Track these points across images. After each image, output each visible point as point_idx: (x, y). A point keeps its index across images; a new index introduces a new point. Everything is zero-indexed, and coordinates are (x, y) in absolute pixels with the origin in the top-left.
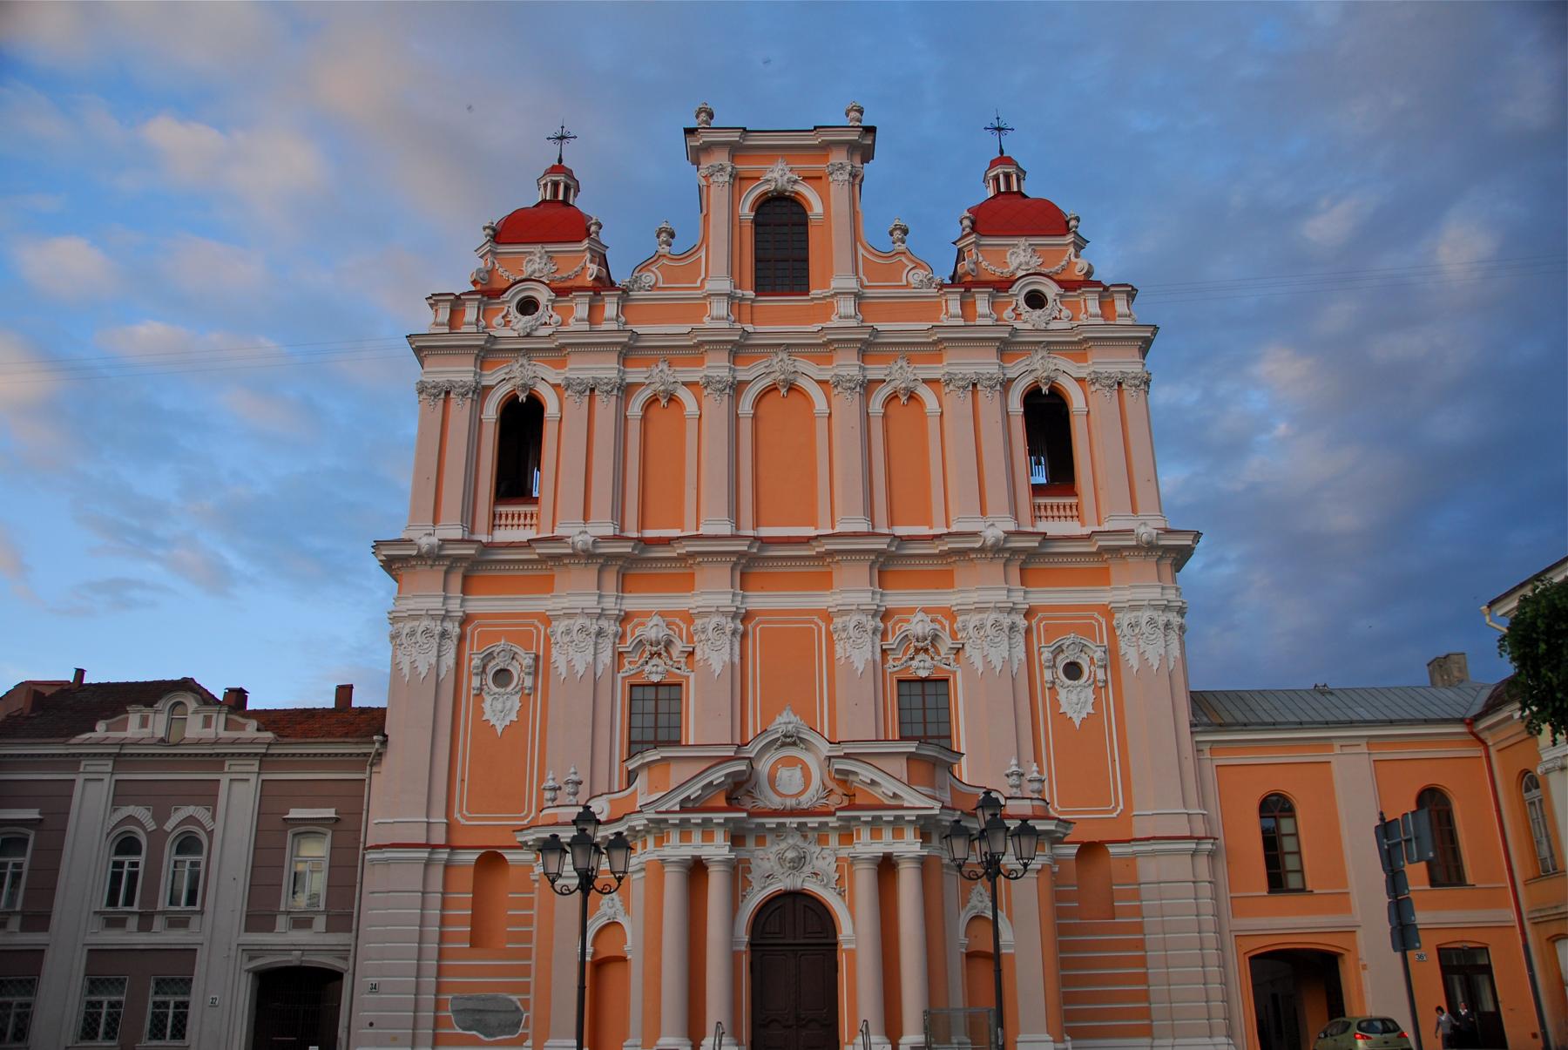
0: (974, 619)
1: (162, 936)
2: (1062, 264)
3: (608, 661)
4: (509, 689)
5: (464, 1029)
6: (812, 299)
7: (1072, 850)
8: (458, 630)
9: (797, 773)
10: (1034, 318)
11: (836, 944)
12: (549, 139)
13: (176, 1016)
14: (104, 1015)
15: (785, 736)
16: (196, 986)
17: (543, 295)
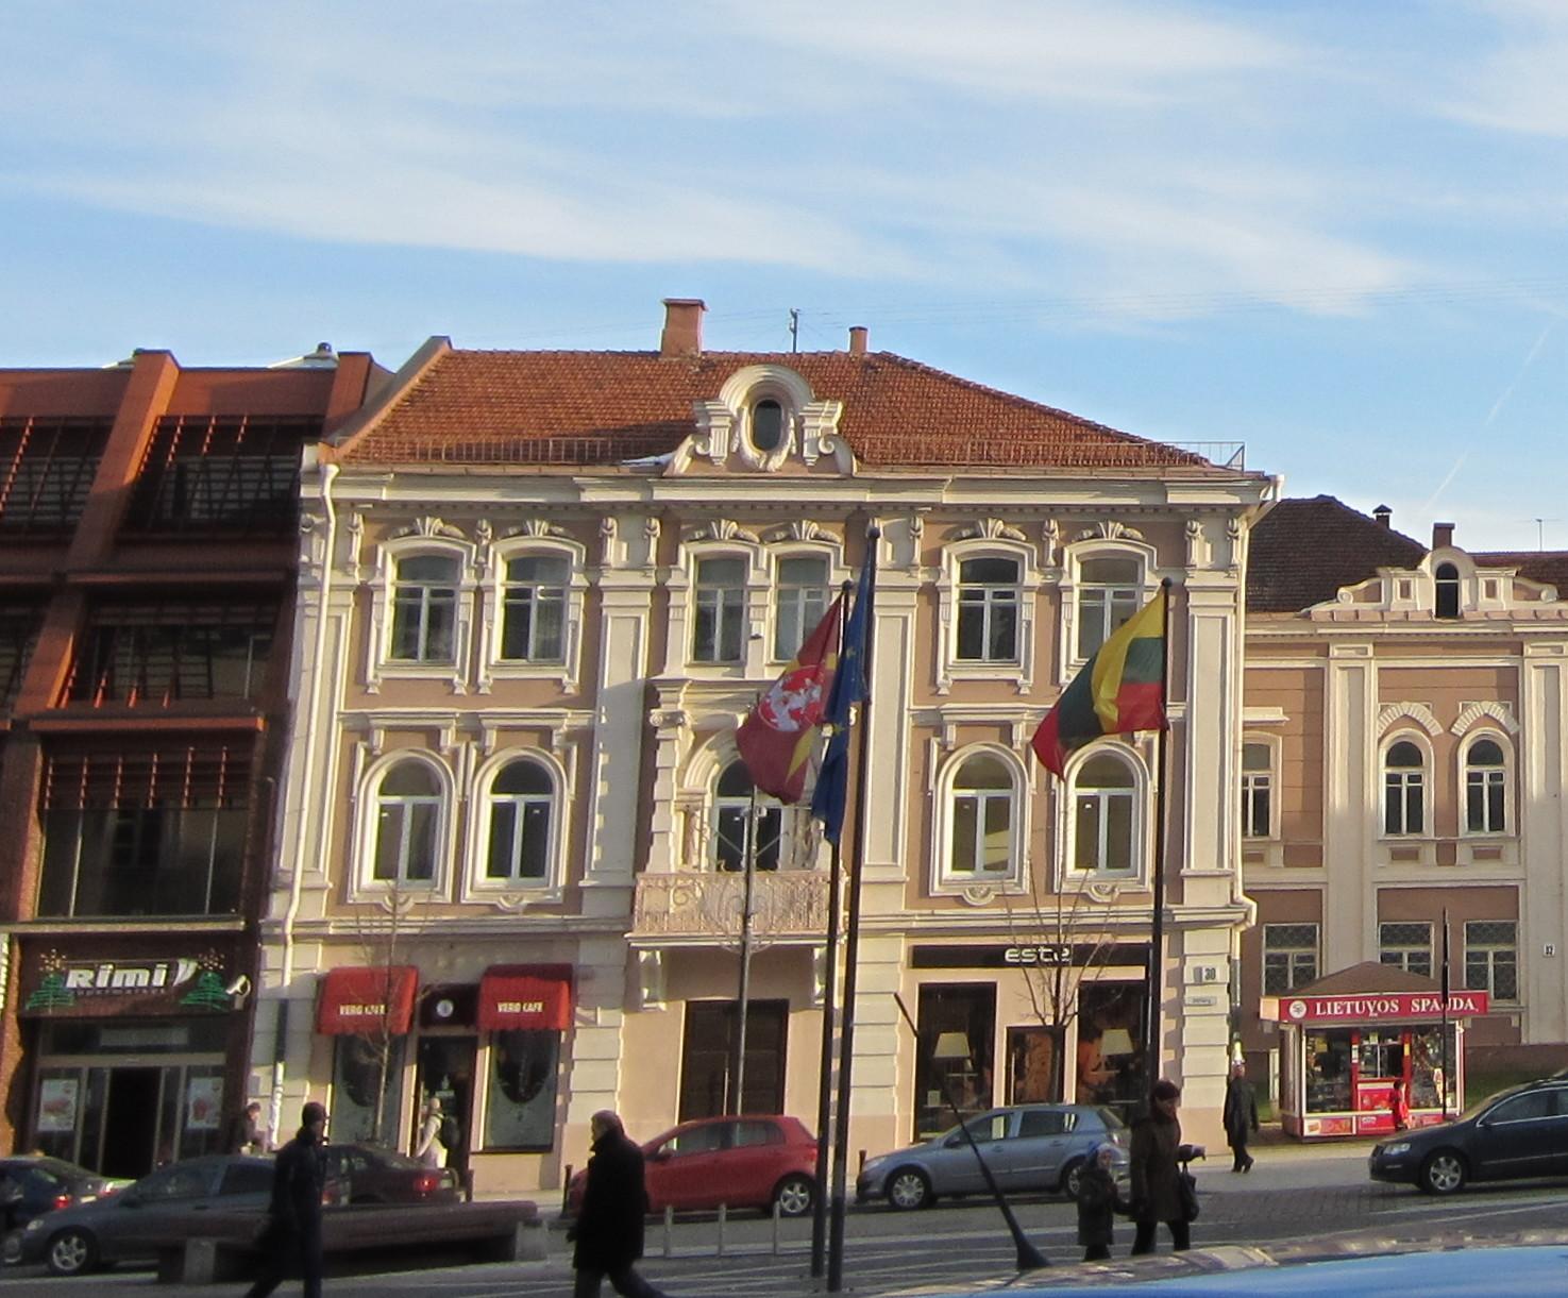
1: (1468, 871)
14: (1491, 969)
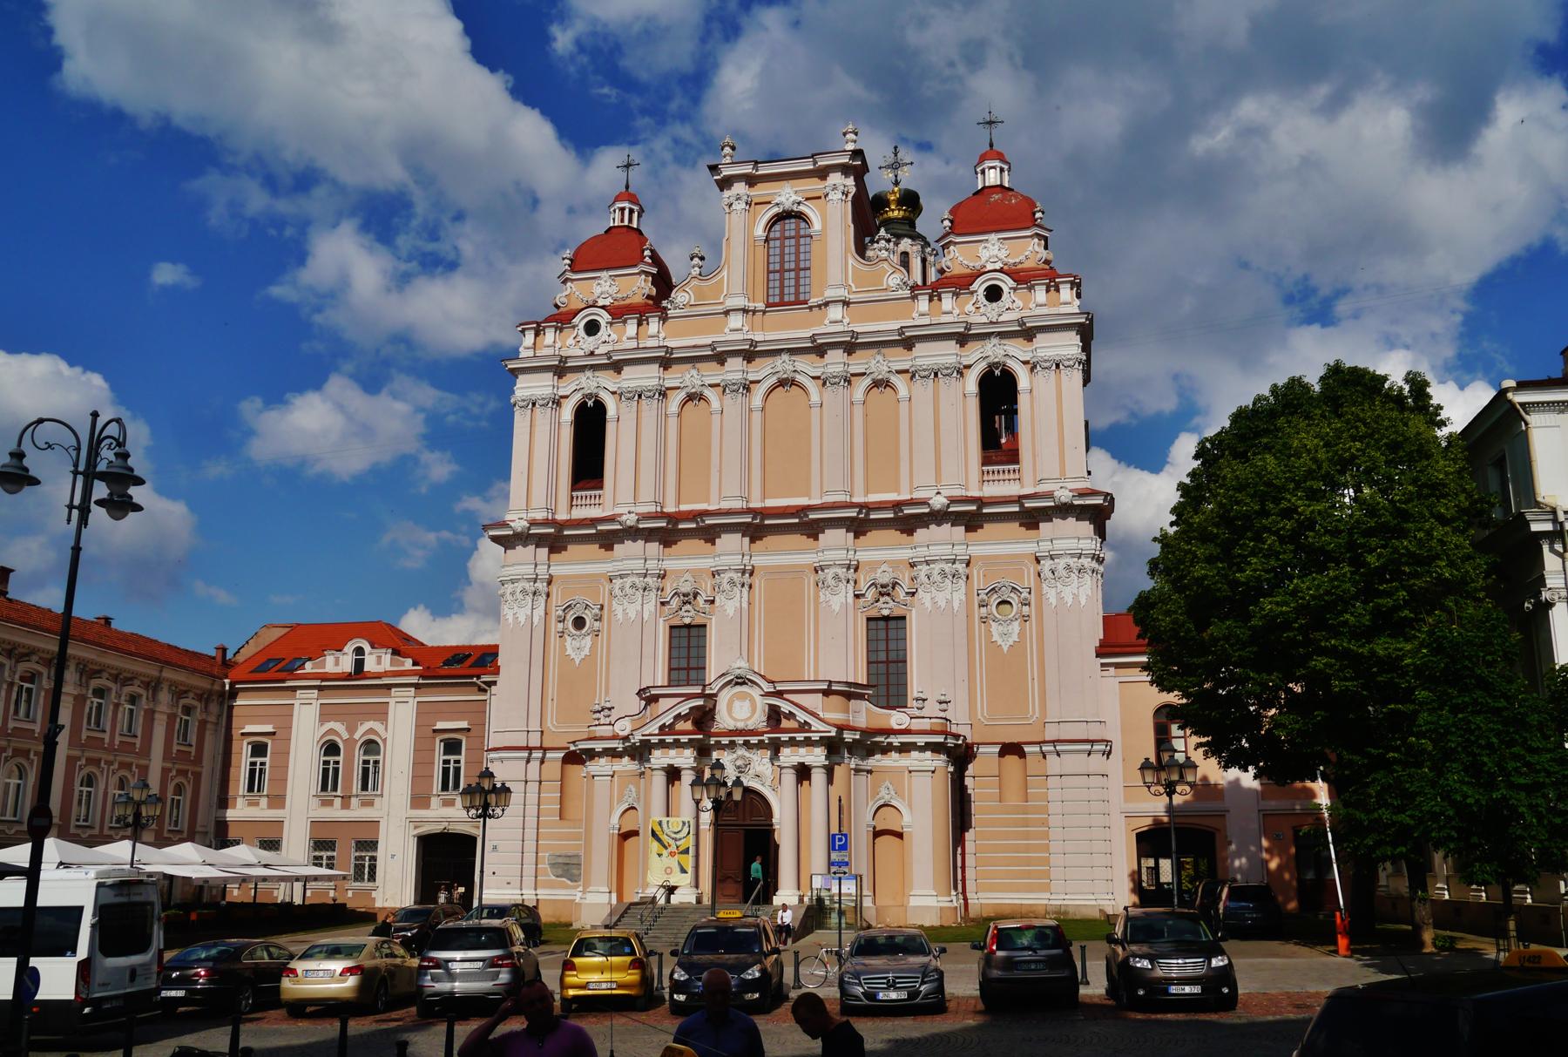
0: (924, 569)
1: (357, 812)
2: (1027, 253)
3: (653, 609)
4: (584, 631)
5: (557, 876)
6: (811, 308)
7: (997, 749)
8: (546, 589)
9: (747, 704)
10: (992, 311)
11: (772, 825)
12: (618, 167)
13: (369, 866)
15: (737, 678)
16: (380, 846)
17: (604, 318)
